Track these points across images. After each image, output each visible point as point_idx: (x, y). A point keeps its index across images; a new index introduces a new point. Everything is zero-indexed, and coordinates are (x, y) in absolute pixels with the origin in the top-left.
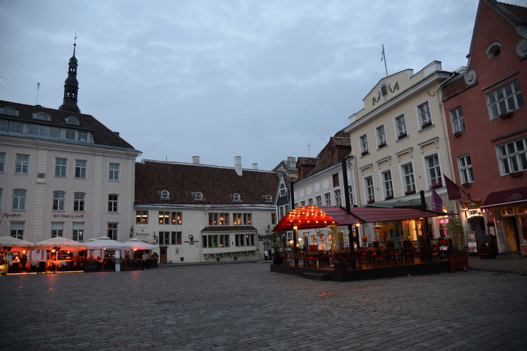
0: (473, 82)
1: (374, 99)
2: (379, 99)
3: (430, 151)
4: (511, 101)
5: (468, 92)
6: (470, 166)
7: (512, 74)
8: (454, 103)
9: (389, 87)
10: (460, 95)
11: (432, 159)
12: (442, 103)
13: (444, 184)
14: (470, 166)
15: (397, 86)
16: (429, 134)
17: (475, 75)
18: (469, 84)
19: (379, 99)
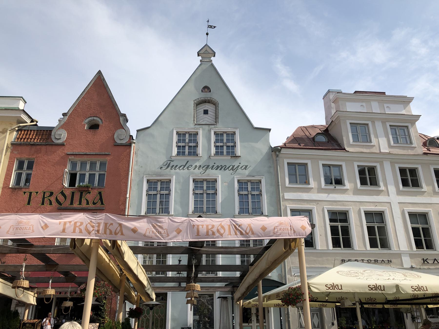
4: (92, 176)
5: (49, 148)
7: (104, 153)
10: (38, 147)
12: (10, 146)
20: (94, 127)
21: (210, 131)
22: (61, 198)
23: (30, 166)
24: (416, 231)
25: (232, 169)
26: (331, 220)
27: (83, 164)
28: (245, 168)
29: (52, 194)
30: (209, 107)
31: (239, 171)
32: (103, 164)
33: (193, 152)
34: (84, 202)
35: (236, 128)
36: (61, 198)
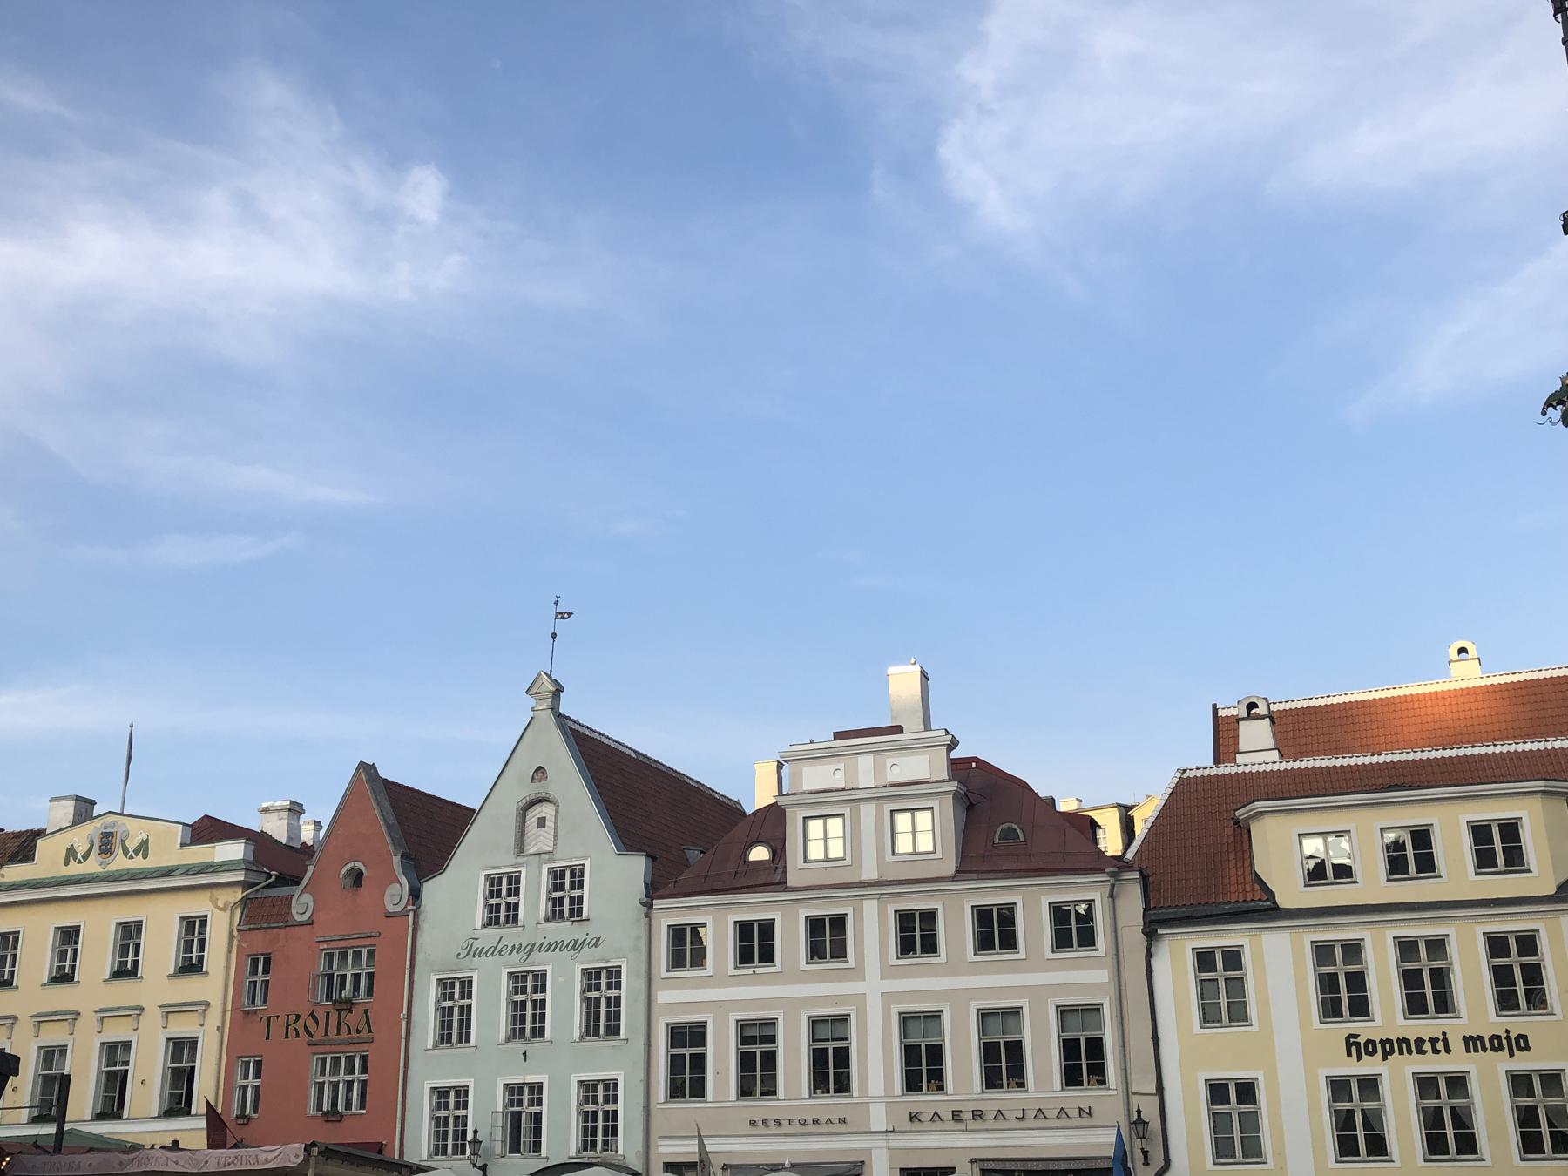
0: (306, 917)
1: (71, 851)
2: (86, 856)
3: (182, 1027)
4: (357, 977)
6: (257, 1082)
8: (259, 942)
9: (123, 842)
11: (182, 1048)
13: (198, 1105)
14: (257, 1082)
15: (143, 849)
16: (191, 989)
17: (311, 905)
18: (298, 918)
19: (86, 856)
20: (357, 878)
21: (540, 868)
22: (311, 1025)
23: (266, 971)
24: (911, 1054)
25: (574, 948)
26: (744, 1040)
27: (344, 956)
28: (596, 945)
29: (298, 1017)
30: (545, 810)
31: (586, 949)
32: (371, 954)
33: (513, 919)
34: (344, 1028)
35: (585, 858)
36: (311, 1025)
